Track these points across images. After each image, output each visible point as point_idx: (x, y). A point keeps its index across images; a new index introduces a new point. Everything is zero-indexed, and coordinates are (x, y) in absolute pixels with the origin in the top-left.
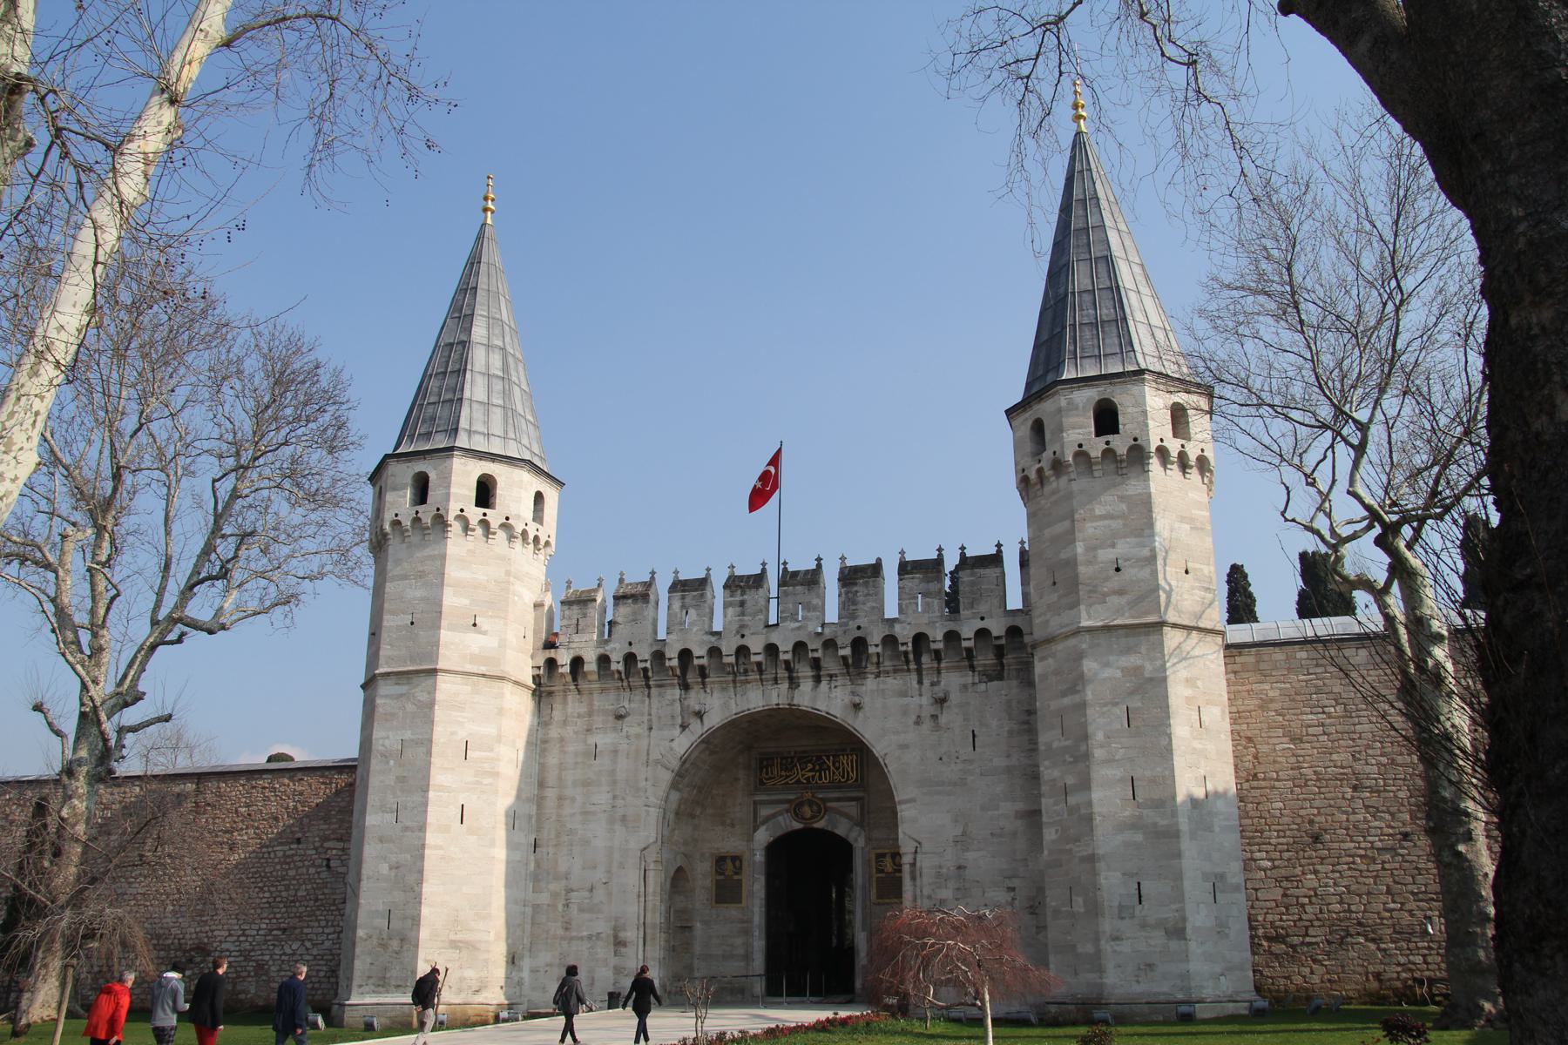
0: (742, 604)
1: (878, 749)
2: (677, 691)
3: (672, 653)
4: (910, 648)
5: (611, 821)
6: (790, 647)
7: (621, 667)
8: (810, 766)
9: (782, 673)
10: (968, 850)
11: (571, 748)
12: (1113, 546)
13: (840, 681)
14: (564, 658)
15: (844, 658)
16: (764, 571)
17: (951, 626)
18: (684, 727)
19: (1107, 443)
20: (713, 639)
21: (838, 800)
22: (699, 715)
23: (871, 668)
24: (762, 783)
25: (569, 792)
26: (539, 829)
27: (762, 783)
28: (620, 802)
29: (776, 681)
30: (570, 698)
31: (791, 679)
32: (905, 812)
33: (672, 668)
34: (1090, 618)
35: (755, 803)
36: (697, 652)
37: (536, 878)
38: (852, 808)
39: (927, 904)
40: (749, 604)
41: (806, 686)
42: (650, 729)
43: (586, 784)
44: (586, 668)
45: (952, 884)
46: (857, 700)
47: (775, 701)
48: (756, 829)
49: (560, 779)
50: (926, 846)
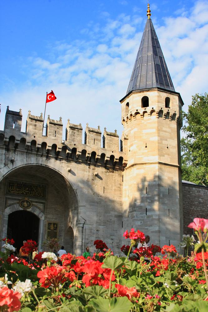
0: (35, 125)
2: (4, 151)
4: (90, 156)
8: (27, 189)
10: (100, 225)
12: (166, 140)
13: (64, 161)
16: (41, 116)
17: (103, 152)
18: (6, 165)
19: (168, 110)
21: (36, 202)
22: (12, 161)
27: (9, 191)
29: (42, 156)
33: (5, 142)
34: (160, 160)
35: (6, 198)
38: (41, 206)
40: (37, 126)
41: (53, 160)
45: (95, 236)
46: (69, 169)
47: (40, 163)
48: (6, 208)
50: (87, 222)
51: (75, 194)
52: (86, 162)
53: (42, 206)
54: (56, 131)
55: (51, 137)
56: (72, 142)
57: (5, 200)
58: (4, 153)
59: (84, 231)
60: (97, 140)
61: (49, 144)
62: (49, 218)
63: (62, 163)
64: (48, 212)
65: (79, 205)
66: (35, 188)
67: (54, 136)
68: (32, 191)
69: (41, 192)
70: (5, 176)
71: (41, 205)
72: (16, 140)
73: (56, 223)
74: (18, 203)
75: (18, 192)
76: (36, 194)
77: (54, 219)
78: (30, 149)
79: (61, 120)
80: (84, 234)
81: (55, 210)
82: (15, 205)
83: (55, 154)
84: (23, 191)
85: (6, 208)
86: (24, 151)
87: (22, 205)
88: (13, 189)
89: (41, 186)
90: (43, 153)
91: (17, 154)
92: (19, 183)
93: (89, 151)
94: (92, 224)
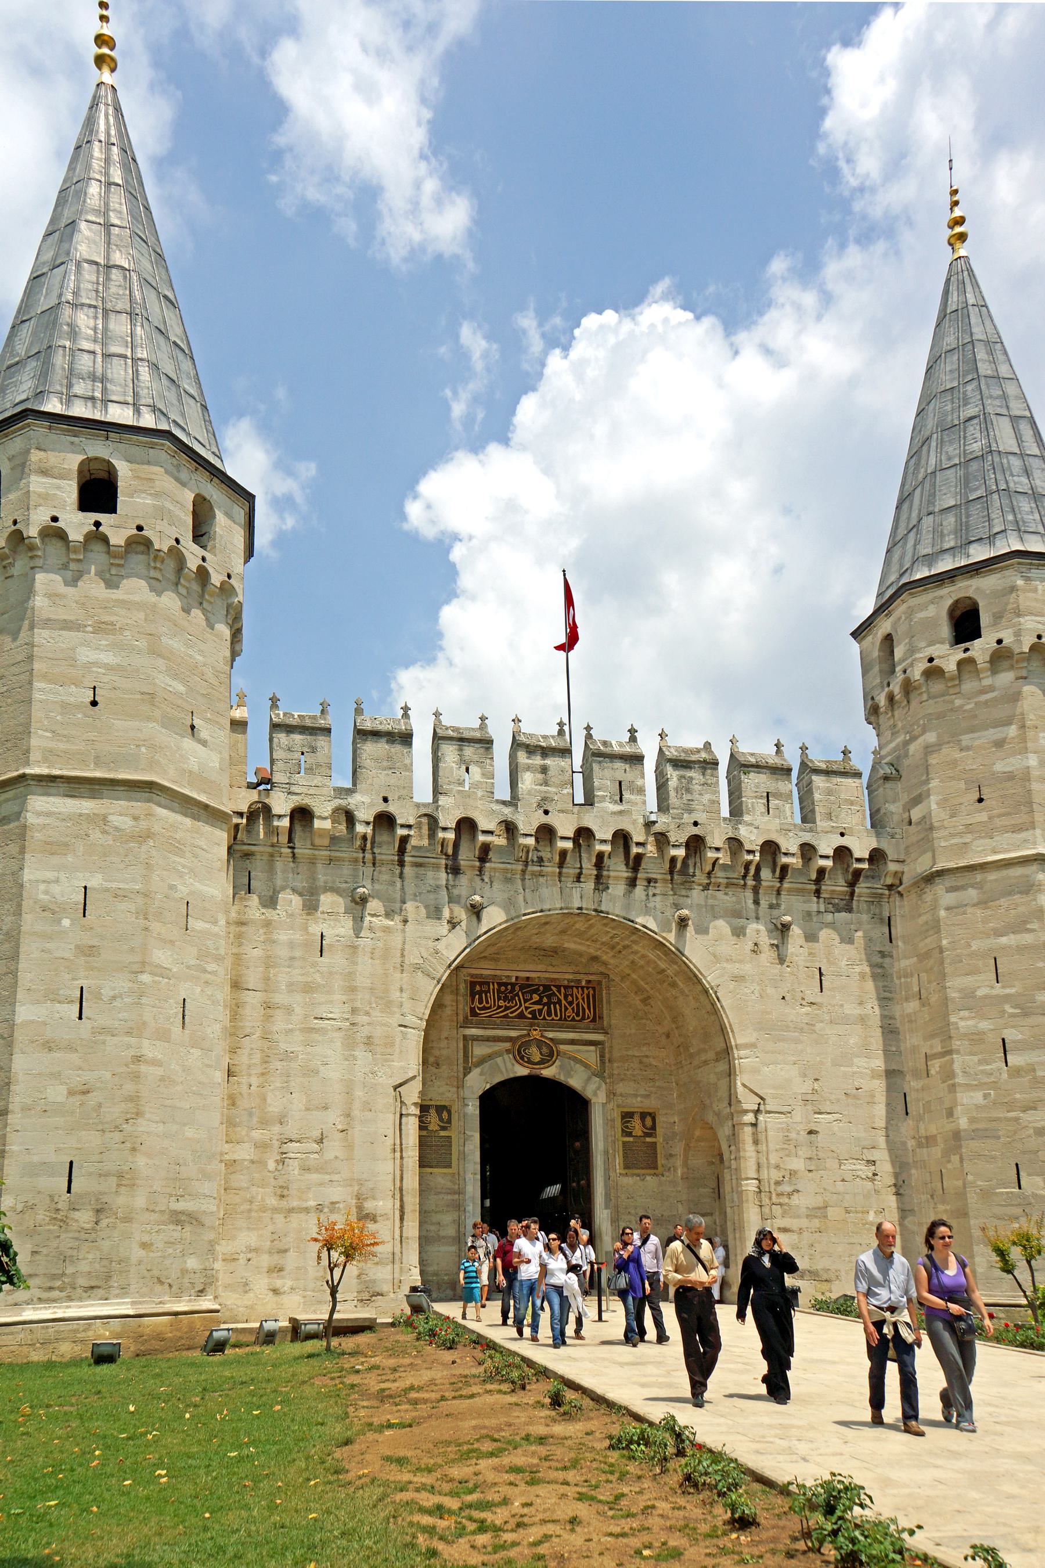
0: (544, 770)
1: (711, 978)
3: (448, 819)
4: (758, 858)
5: (350, 1044)
6: (609, 836)
7: (369, 830)
8: (536, 997)
9: (589, 866)
11: (283, 936)
14: (281, 804)
15: (673, 860)
18: (453, 924)
20: (507, 811)
21: (573, 1042)
23: (700, 878)
24: (474, 1013)
25: (281, 998)
26: (233, 1051)
28: (362, 1019)
30: (279, 865)
31: (598, 877)
32: (744, 1060)
35: (465, 1037)
36: (483, 824)
37: (231, 1123)
38: (590, 1055)
39: (776, 1175)
41: (617, 889)
42: (405, 921)
43: (308, 988)
44: (317, 824)
45: (803, 1152)
47: (577, 904)
49: (267, 979)
51: (713, 1004)
52: (742, 882)
54: (620, 783)
55: (603, 805)
56: (685, 816)
57: (461, 1045)
58: (444, 883)
59: (762, 1137)
60: (779, 795)
61: (604, 832)
62: (621, 1095)
63: (654, 895)
64: (619, 1074)
65: (733, 1043)
66: (563, 990)
67: (616, 802)
68: (555, 1004)
69: (585, 1006)
70: (456, 963)
72: (480, 833)
73: (651, 1111)
74: (508, 1051)
77: (642, 1096)
78: (535, 859)
79: (633, 739)
80: (763, 1147)
81: (641, 1062)
82: (499, 1060)
83: (627, 865)
86: (514, 867)
87: (522, 1058)
88: (487, 1002)
89: (583, 983)
90: (581, 868)
91: (492, 882)
93: (752, 838)
94: (789, 1109)
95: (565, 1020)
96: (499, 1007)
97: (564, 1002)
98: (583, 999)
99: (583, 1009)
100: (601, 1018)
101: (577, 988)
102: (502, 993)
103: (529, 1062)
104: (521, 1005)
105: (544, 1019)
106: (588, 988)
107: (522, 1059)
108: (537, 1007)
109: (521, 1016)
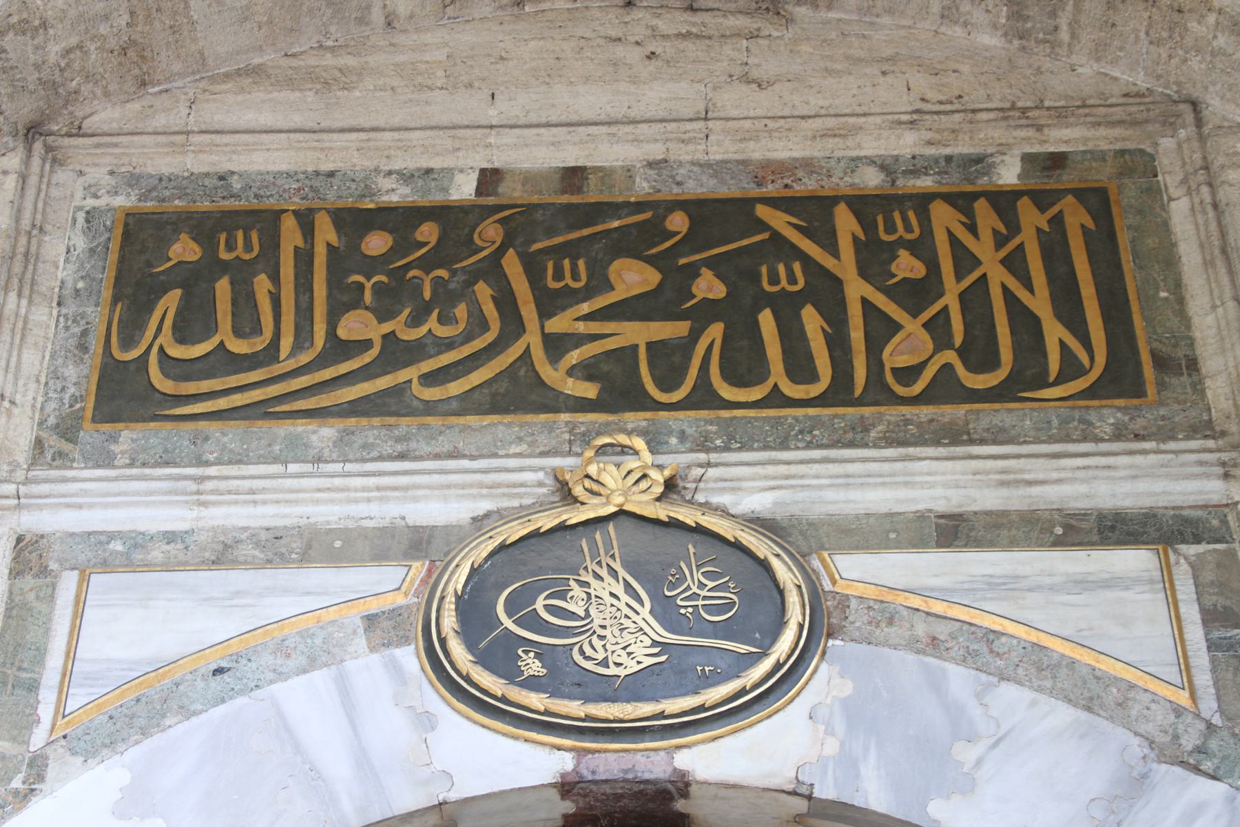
53: (1152, 604)
66: (846, 223)
69: (1040, 303)
71: (1083, 584)
75: (384, 382)
76: (896, 355)
82: (303, 698)
84: (532, 339)
85: (24, 797)
88: (246, 324)
92: (396, 194)
95: (878, 392)
96: (339, 349)
97: (856, 289)
98: (1015, 263)
99: (1026, 325)
100: (1180, 364)
101: (962, 202)
102: (371, 265)
103: (562, 676)
104: (513, 325)
105: (704, 398)
106: (1042, 199)
107: (507, 668)
108: (636, 333)
109: (520, 395)
